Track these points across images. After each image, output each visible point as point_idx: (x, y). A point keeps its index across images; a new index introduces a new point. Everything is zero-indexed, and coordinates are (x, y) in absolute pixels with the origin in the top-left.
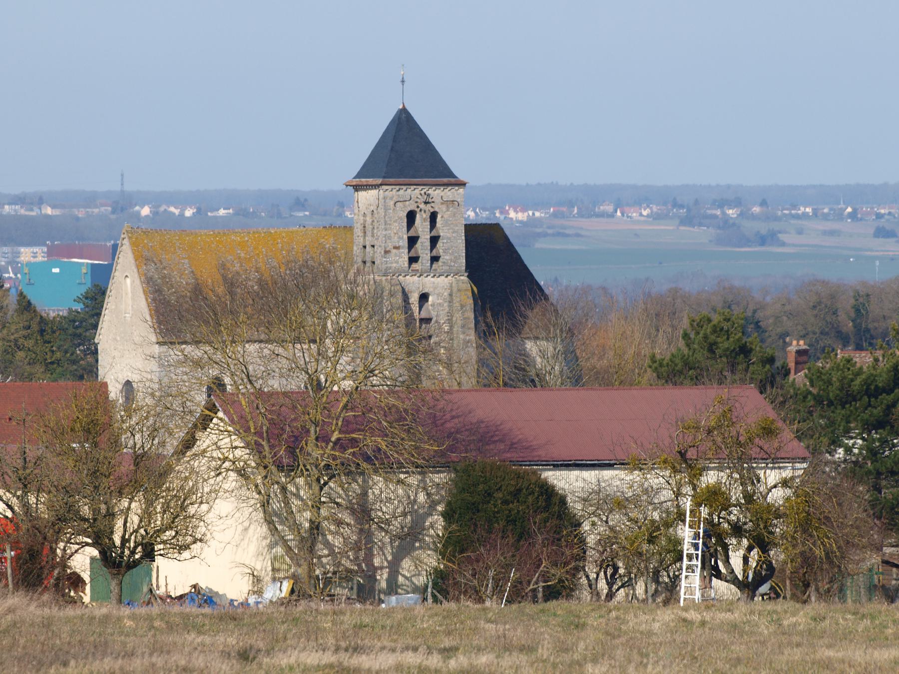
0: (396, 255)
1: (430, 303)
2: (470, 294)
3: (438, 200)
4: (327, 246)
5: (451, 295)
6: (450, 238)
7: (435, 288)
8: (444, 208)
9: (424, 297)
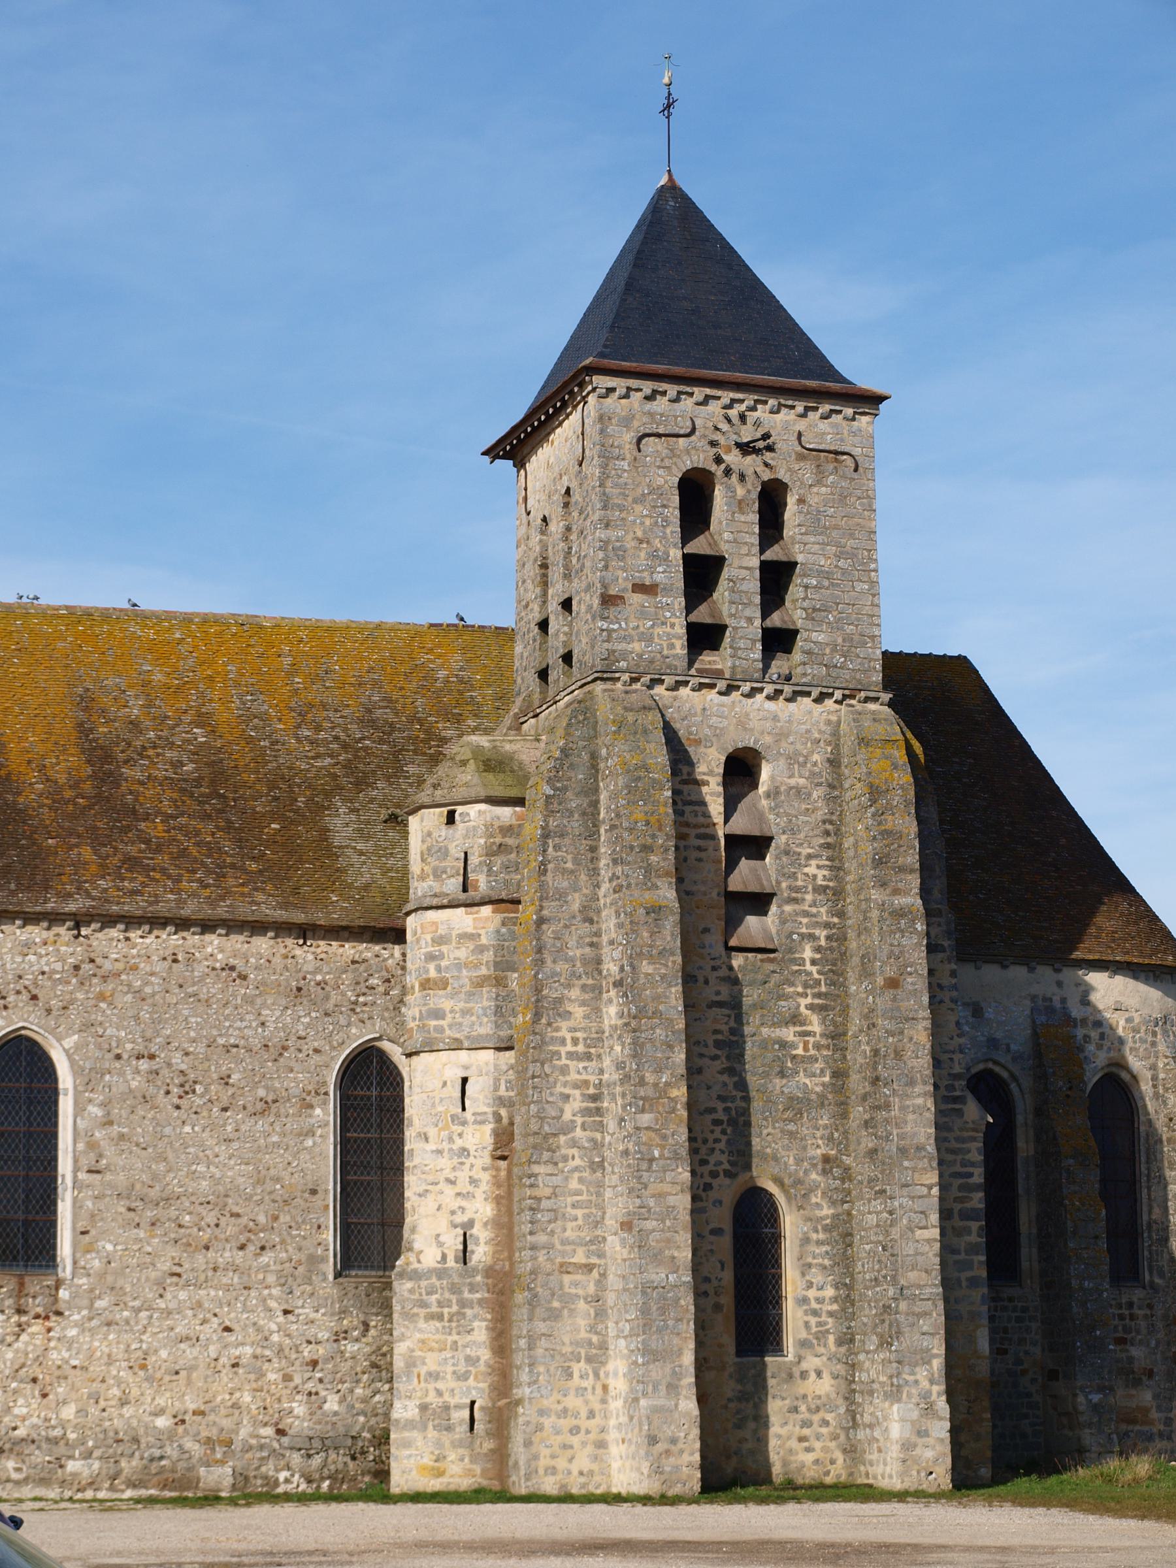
0: (642, 614)
1: (762, 789)
2: (901, 756)
4: (442, 674)
5: (834, 762)
6: (828, 575)
7: (781, 736)
8: (807, 472)
9: (741, 769)
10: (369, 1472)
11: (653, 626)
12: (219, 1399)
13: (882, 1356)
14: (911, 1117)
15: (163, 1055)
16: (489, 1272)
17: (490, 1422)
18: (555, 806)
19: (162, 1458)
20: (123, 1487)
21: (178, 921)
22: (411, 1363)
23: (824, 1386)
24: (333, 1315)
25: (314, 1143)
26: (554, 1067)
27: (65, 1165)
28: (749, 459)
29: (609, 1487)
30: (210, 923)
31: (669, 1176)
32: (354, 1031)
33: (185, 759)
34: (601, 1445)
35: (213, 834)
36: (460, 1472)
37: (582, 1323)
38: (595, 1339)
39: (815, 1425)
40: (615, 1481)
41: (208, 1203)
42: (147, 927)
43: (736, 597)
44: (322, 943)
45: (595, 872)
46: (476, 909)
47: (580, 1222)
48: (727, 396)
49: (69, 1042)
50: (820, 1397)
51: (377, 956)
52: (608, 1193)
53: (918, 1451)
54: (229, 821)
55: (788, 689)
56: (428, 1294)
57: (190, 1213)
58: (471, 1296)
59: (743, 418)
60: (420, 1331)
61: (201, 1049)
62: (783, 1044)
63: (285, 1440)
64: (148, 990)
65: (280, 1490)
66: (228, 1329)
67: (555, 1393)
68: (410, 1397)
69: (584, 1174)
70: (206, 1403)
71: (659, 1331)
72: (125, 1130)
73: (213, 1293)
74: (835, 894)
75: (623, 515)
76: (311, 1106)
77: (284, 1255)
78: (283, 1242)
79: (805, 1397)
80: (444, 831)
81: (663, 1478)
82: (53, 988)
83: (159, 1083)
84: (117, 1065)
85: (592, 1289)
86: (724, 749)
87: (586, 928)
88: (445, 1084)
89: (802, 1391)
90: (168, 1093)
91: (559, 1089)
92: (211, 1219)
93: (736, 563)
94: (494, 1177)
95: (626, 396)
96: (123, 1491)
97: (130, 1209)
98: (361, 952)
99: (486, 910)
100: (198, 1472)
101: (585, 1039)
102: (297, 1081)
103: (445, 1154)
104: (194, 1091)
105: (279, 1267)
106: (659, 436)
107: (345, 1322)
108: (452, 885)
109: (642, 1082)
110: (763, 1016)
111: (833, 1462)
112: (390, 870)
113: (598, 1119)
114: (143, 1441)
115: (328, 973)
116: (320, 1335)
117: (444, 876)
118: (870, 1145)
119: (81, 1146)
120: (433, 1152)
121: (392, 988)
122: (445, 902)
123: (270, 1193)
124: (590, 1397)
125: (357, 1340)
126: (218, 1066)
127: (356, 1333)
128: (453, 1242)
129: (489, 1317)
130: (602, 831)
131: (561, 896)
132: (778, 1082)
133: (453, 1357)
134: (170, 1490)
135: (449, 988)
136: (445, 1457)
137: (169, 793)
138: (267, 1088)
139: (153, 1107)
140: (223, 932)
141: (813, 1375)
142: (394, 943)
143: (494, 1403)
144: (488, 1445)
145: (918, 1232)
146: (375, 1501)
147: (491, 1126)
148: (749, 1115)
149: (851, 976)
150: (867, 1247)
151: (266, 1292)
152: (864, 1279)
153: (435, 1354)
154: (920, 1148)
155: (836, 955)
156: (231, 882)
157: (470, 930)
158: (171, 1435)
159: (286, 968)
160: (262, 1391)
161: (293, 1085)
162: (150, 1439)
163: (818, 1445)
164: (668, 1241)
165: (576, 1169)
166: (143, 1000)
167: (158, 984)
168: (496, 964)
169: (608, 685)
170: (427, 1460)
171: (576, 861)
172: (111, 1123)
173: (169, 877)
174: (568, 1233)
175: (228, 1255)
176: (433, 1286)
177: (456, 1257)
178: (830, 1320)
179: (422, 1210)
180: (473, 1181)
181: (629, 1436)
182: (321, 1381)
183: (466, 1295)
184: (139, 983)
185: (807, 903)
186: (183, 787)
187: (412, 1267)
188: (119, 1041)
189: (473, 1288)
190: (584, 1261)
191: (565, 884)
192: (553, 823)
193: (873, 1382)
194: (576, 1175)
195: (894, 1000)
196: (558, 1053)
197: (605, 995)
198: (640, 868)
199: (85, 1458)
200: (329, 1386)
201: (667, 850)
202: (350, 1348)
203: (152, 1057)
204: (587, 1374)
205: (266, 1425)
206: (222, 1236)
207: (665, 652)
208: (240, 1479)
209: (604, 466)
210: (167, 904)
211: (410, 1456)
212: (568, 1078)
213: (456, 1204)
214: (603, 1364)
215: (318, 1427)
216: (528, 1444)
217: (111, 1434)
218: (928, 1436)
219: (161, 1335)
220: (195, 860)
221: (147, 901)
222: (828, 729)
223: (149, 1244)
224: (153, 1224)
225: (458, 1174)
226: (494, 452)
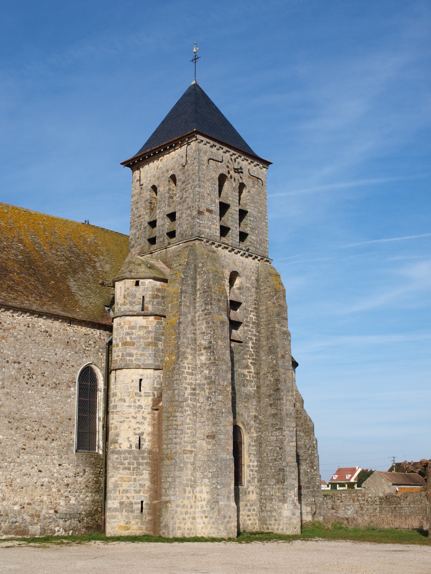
0: (209, 220)
3: (245, 172)
5: (257, 280)
6: (255, 218)
10: (85, 527)
12: (36, 498)
13: (278, 486)
14: (288, 403)
16: (150, 452)
17: (149, 509)
18: (184, 282)
19: (16, 522)
20: (2, 534)
21: (31, 312)
22: (116, 486)
23: (253, 497)
24: (74, 466)
25: (71, 401)
26: (182, 377)
28: (236, 174)
29: (196, 534)
30: (41, 314)
31: (227, 419)
32: (84, 360)
34: (194, 518)
35: (34, 282)
36: (136, 528)
37: (189, 472)
38: (193, 478)
39: (252, 511)
40: (198, 532)
41: (36, 421)
42: (20, 312)
43: (233, 219)
44: (76, 326)
45: (195, 308)
46: (147, 317)
47: (189, 435)
48: (232, 152)
50: (252, 501)
52: (198, 425)
53: (293, 521)
54: (37, 278)
55: (247, 253)
56: (124, 460)
58: (143, 461)
59: (235, 160)
60: (120, 474)
61: (35, 361)
62: (244, 375)
63: (58, 515)
64: (19, 337)
65: (56, 535)
66: (40, 471)
67: (181, 499)
68: (115, 499)
69: (191, 417)
70: (32, 500)
71: (225, 476)
72: (9, 391)
73: (36, 457)
74: (257, 325)
75: (204, 184)
76: (70, 387)
77: (59, 443)
78: (60, 438)
79: (249, 500)
80: (134, 288)
81: (228, 531)
83: (21, 373)
85: (192, 460)
86: (230, 270)
87: (192, 328)
88: (133, 381)
89: (248, 499)
90: (24, 377)
92: (36, 428)
93: (233, 209)
94: (152, 416)
95: (205, 144)
96: (2, 536)
97: (9, 422)
98: (87, 331)
99: (152, 318)
100: (28, 528)
101: (192, 367)
102: (65, 377)
104: (33, 378)
105: (58, 448)
106: (214, 160)
107: (78, 469)
108: (138, 308)
109: (219, 384)
110: (239, 365)
111: (256, 524)
113: (195, 397)
115: (77, 337)
116: (70, 474)
117: (134, 304)
118: (273, 412)
120: (127, 406)
121: (96, 345)
122: (135, 314)
123: (56, 419)
124: (191, 500)
126: (41, 369)
127: (81, 474)
128: (135, 440)
129: (150, 469)
130: (198, 293)
131: (185, 314)
133: (134, 484)
134: (19, 535)
135: (135, 345)
136: (130, 523)
137: (16, 265)
140: (45, 318)
141: (251, 492)
142: (98, 329)
143: (151, 502)
144: (149, 518)
145: (291, 443)
146: (141, 541)
147: (152, 398)
148: (236, 400)
149: (262, 353)
150: (270, 448)
151: (53, 457)
152: (268, 459)
153: (127, 483)
154: (291, 414)
155: (257, 346)
156: (45, 300)
157: (144, 325)
158: (19, 513)
159: (64, 334)
160: (50, 496)
161: (65, 378)
162: (12, 514)
163: (252, 518)
164: (227, 443)
165: (189, 415)
166: (17, 340)
167: (22, 335)
168: (155, 338)
169: (200, 242)
170: (122, 524)
171: (190, 303)
172: (4, 387)
173: (25, 295)
174: (186, 439)
175: (41, 442)
176: (126, 457)
177: (136, 446)
178: (256, 473)
179: (122, 428)
180: (144, 418)
181: (211, 515)
182: (70, 492)
183: (140, 460)
184: (16, 334)
185: (250, 327)
188: (8, 355)
189: (143, 458)
190: (190, 449)
191: (187, 311)
192: (184, 288)
194: (189, 417)
195: (283, 362)
196: (183, 372)
197: (198, 352)
198: (217, 307)
201: (224, 302)
202: (79, 479)
203: (19, 363)
204: (191, 492)
205: (51, 509)
206: (40, 435)
207: (214, 234)
208: (43, 530)
209: (199, 166)
210: (26, 304)
211: (115, 522)
212: (187, 381)
214: (195, 488)
215: (68, 510)
216: (173, 518)
218: (295, 515)
219: (17, 473)
220: (31, 290)
221: (20, 303)
223: (15, 436)
224: (17, 429)
226: (127, 164)
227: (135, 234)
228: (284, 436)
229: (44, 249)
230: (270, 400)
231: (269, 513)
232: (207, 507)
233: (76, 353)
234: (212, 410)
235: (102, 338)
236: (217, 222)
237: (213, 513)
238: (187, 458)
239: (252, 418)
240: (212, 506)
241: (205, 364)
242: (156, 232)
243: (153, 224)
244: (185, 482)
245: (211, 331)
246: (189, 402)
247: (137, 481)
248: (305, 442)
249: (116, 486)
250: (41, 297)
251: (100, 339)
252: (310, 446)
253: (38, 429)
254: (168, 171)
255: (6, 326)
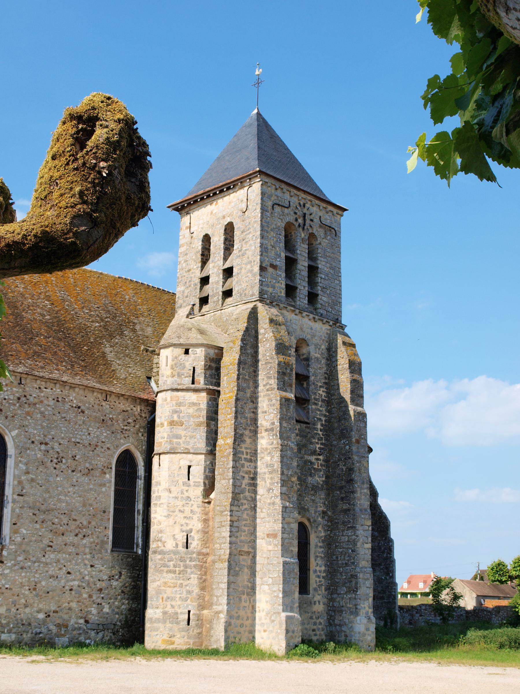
11: (275, 283)
12: (64, 605)
14: (363, 497)
15: (50, 444)
19: (40, 633)
24: (109, 568)
25: (106, 490)
27: (8, 491)
30: (73, 386)
33: (45, 313)
36: (181, 642)
37: (246, 578)
39: (318, 624)
41: (65, 514)
47: (246, 533)
49: (15, 433)
50: (319, 612)
51: (132, 409)
53: (366, 637)
56: (168, 561)
57: (57, 518)
60: (164, 578)
61: (64, 442)
62: (312, 463)
66: (69, 573)
70: (58, 607)
73: (64, 555)
75: (268, 235)
76: (105, 473)
77: (92, 540)
78: (92, 534)
82: (9, 407)
83: (48, 456)
84: (32, 446)
85: (249, 562)
87: (251, 405)
88: (180, 467)
91: (241, 474)
93: (301, 263)
97: (34, 514)
100: (55, 640)
101: (250, 453)
102: (100, 461)
103: (179, 499)
104: (62, 461)
106: (279, 205)
107: (113, 572)
112: (131, 374)
113: (254, 488)
114: (33, 624)
115: (114, 415)
116: (104, 577)
117: (183, 376)
118: (344, 507)
119: (16, 483)
120: (173, 497)
122: (184, 388)
125: (117, 580)
127: (117, 577)
132: (310, 479)
133: (180, 590)
137: (43, 327)
138: (90, 463)
139: (46, 467)
141: (317, 603)
145: (365, 545)
150: (340, 550)
151: (85, 556)
153: (171, 589)
154: (366, 510)
155: (327, 428)
157: (195, 401)
158: (44, 622)
159: (99, 410)
163: (318, 633)
164: (291, 543)
165: (246, 509)
167: (51, 411)
170: (166, 637)
172: (28, 473)
175: (70, 538)
177: (183, 545)
181: (271, 629)
182: (103, 598)
185: (319, 406)
186: (49, 326)
187: (161, 549)
190: (247, 550)
193: (343, 606)
194: (246, 512)
195: (358, 448)
196: (241, 458)
199: (9, 633)
200: (105, 601)
202: (115, 583)
203: (46, 444)
206: (69, 530)
207: (279, 294)
213: (184, 521)
215: (101, 619)
217: (20, 621)
218: (369, 630)
219: (43, 575)
222: (327, 336)
224: (43, 522)
225: (185, 508)
227: (183, 292)
228: (357, 536)
229: (76, 308)
230: (341, 493)
231: (337, 627)
232: (266, 619)
233: (113, 433)
234: (274, 503)
235: (143, 415)
236: (282, 279)
237: (273, 627)
238: (244, 560)
239: (320, 514)
240: (273, 618)
241: (267, 449)
242: (208, 289)
243: (205, 281)
244: (240, 589)
245: (274, 410)
246: (247, 494)
247: (184, 587)
248: (379, 543)
249: (158, 592)
250: (73, 366)
251: (141, 416)
252: (385, 549)
253: (67, 522)
254: (224, 217)
255: (31, 399)
